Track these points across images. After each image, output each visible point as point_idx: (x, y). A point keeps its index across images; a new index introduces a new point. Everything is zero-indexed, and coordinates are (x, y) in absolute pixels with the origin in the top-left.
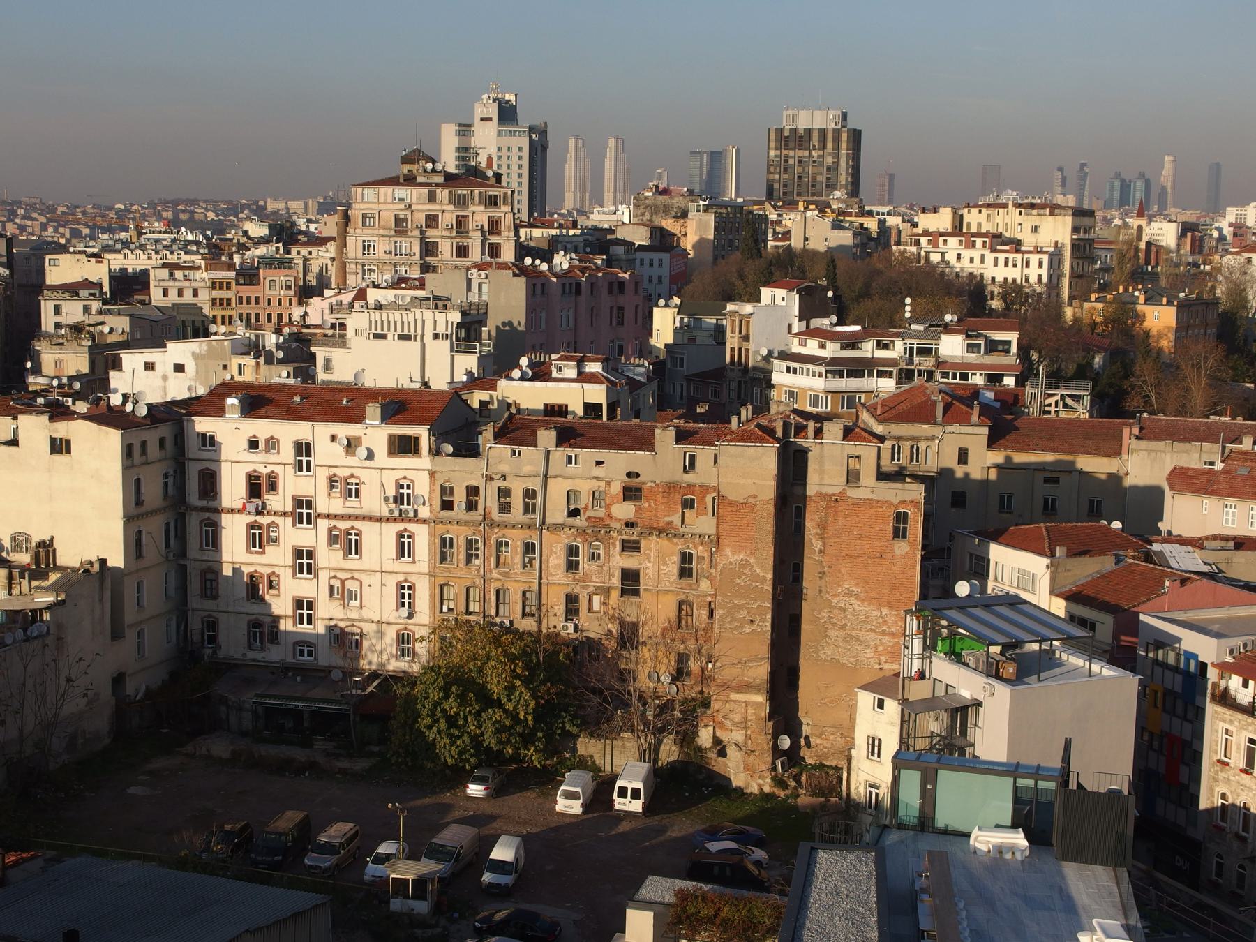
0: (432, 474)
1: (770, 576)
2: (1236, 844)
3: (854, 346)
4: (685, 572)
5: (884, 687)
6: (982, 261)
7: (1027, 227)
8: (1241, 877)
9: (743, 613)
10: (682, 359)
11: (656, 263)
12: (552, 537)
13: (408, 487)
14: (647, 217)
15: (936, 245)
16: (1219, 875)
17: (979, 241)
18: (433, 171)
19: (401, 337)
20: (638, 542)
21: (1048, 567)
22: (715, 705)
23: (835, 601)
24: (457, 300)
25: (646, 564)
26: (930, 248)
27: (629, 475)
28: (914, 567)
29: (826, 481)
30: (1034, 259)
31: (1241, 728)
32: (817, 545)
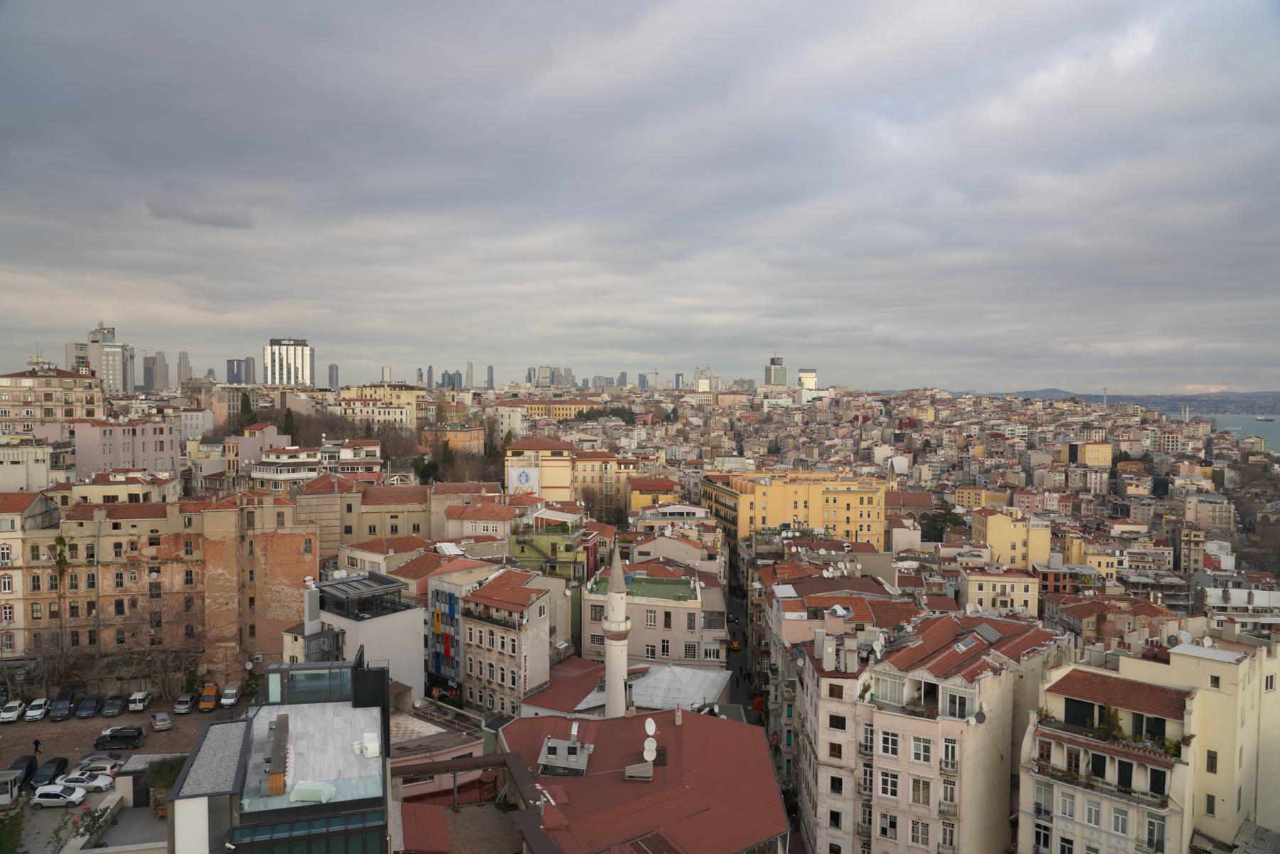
0: (24, 541)
1: (235, 579)
2: (477, 682)
3: (295, 457)
4: (189, 580)
5: (297, 630)
6: (373, 413)
7: (394, 396)
8: (481, 697)
9: (221, 600)
10: (201, 468)
11: (194, 418)
12: (106, 569)
13: (7, 549)
14: (189, 393)
15: (349, 406)
16: (471, 697)
17: (371, 404)
18: (49, 369)
19: (13, 463)
20: (159, 568)
21: (385, 559)
22: (208, 651)
23: (274, 588)
24: (50, 441)
25: (164, 579)
26: (346, 407)
27: (152, 531)
28: (316, 566)
29: (266, 526)
30: (398, 411)
31: (475, 626)
32: (262, 560)
